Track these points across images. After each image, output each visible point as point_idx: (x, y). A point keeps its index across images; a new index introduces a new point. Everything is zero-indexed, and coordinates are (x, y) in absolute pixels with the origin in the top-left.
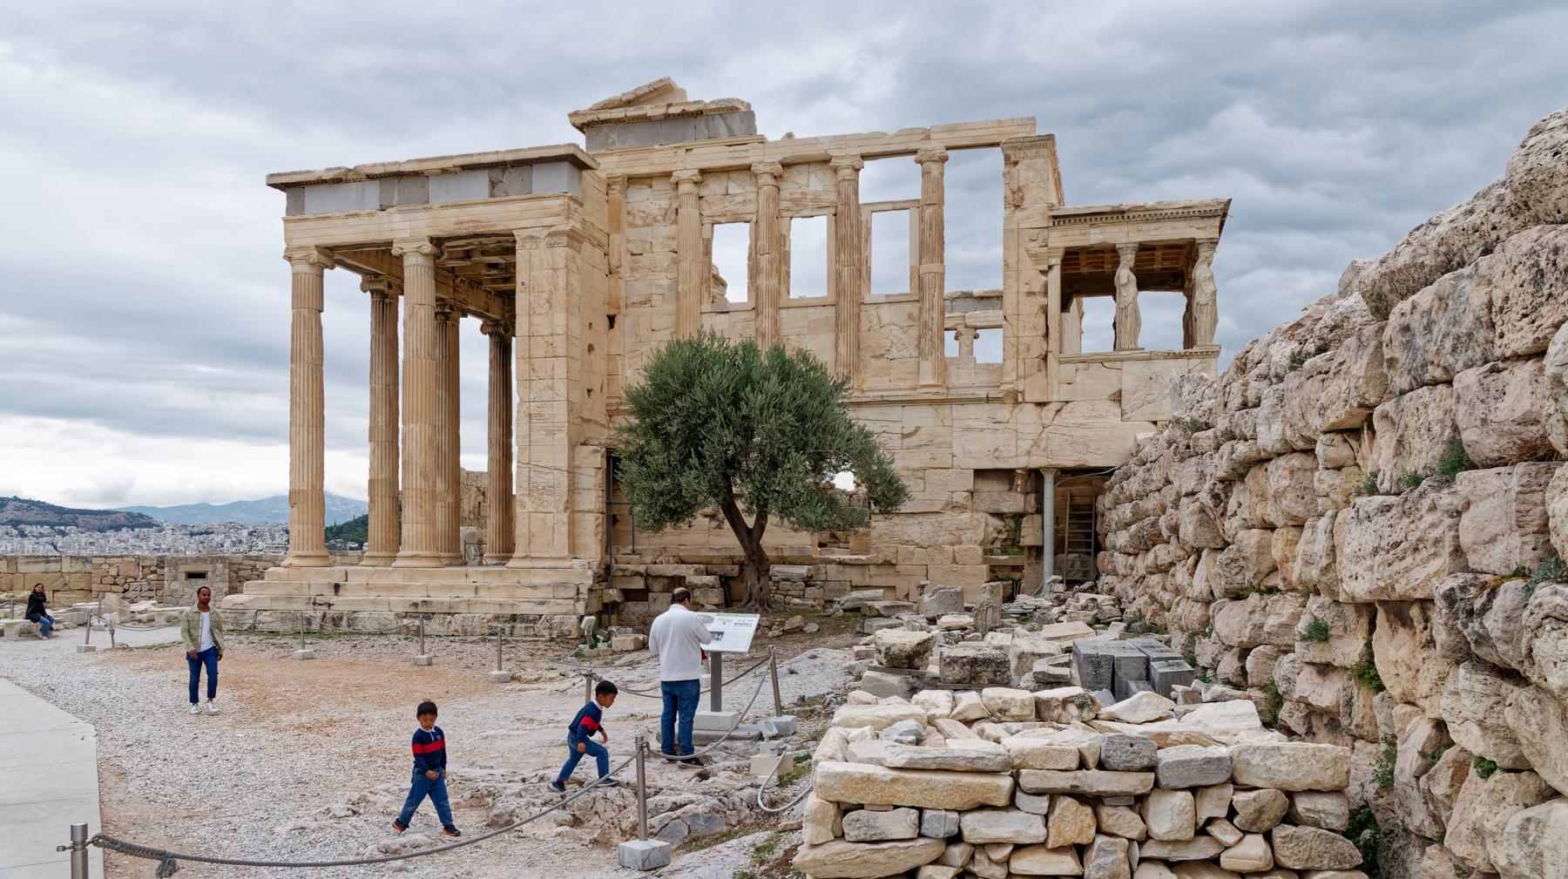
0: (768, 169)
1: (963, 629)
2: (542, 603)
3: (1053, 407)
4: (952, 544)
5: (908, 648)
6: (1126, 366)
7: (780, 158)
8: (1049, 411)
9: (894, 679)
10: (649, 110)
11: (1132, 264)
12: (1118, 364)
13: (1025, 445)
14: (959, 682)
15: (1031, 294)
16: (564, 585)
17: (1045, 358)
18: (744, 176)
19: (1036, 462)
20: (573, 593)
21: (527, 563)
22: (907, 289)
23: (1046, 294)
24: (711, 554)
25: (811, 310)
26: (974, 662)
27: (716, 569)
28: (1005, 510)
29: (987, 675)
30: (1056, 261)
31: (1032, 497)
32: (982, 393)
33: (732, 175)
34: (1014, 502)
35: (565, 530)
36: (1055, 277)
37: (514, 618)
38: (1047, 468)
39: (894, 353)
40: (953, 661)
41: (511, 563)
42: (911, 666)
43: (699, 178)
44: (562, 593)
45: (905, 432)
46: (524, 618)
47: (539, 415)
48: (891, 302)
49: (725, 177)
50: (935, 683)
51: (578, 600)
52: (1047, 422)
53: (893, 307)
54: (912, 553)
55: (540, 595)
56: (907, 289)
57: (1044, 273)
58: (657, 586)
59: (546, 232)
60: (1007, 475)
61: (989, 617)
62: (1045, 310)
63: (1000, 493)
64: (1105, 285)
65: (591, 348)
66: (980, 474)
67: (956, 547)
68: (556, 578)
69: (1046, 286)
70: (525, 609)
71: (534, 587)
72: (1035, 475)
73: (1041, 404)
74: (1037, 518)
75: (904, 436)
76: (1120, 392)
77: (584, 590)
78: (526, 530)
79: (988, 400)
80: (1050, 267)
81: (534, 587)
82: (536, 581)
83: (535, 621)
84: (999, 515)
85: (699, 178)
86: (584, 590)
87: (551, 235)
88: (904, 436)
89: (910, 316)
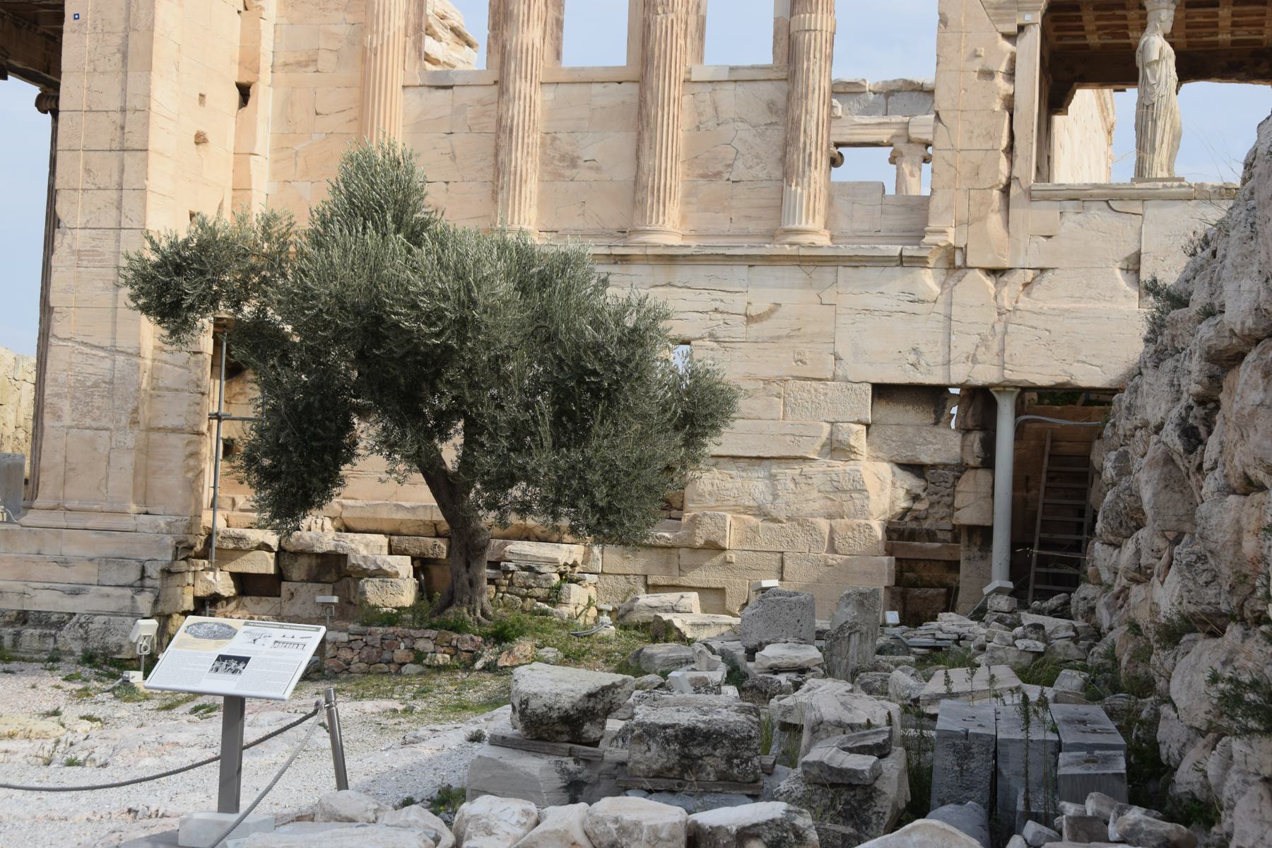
1: (802, 670)
2: (75, 593)
3: (1017, 279)
4: (830, 517)
5: (565, 703)
6: (1152, 211)
8: (1010, 290)
9: (535, 766)
11: (1168, 28)
12: (1136, 207)
13: (963, 345)
14: (658, 775)
16: (120, 561)
19: (984, 375)
20: (133, 576)
21: (58, 519)
22: (768, 59)
23: (1011, 75)
24: (400, 516)
25: (597, 88)
26: (689, 735)
27: (406, 543)
28: (926, 459)
29: (713, 763)
31: (976, 438)
32: (895, 250)
34: (944, 443)
35: (127, 460)
36: (1030, 48)
37: (23, 618)
38: (1004, 387)
39: (740, 171)
40: (649, 732)
41: (30, 518)
42: (577, 738)
44: (115, 575)
45: (753, 311)
46: (42, 620)
48: (738, 77)
50: (622, 781)
51: (141, 589)
52: (1007, 304)
53: (740, 89)
54: (755, 530)
55: (74, 576)
56: (768, 59)
58: (298, 570)
60: (931, 397)
61: (853, 651)
62: (1010, 104)
63: (918, 427)
64: (1119, 68)
65: (200, 139)
66: (882, 392)
67: (837, 522)
68: (109, 547)
69: (1013, 61)
70: (45, 601)
71: (65, 563)
72: (981, 399)
73: (995, 272)
74: (983, 475)
75: (750, 319)
76: (1138, 255)
77: (153, 570)
78: (59, 458)
79: (901, 261)
80: (1021, 28)
81: (65, 563)
82: (72, 551)
83: (60, 625)
84: (915, 469)
86: (153, 570)
88: (750, 319)
89: (771, 106)
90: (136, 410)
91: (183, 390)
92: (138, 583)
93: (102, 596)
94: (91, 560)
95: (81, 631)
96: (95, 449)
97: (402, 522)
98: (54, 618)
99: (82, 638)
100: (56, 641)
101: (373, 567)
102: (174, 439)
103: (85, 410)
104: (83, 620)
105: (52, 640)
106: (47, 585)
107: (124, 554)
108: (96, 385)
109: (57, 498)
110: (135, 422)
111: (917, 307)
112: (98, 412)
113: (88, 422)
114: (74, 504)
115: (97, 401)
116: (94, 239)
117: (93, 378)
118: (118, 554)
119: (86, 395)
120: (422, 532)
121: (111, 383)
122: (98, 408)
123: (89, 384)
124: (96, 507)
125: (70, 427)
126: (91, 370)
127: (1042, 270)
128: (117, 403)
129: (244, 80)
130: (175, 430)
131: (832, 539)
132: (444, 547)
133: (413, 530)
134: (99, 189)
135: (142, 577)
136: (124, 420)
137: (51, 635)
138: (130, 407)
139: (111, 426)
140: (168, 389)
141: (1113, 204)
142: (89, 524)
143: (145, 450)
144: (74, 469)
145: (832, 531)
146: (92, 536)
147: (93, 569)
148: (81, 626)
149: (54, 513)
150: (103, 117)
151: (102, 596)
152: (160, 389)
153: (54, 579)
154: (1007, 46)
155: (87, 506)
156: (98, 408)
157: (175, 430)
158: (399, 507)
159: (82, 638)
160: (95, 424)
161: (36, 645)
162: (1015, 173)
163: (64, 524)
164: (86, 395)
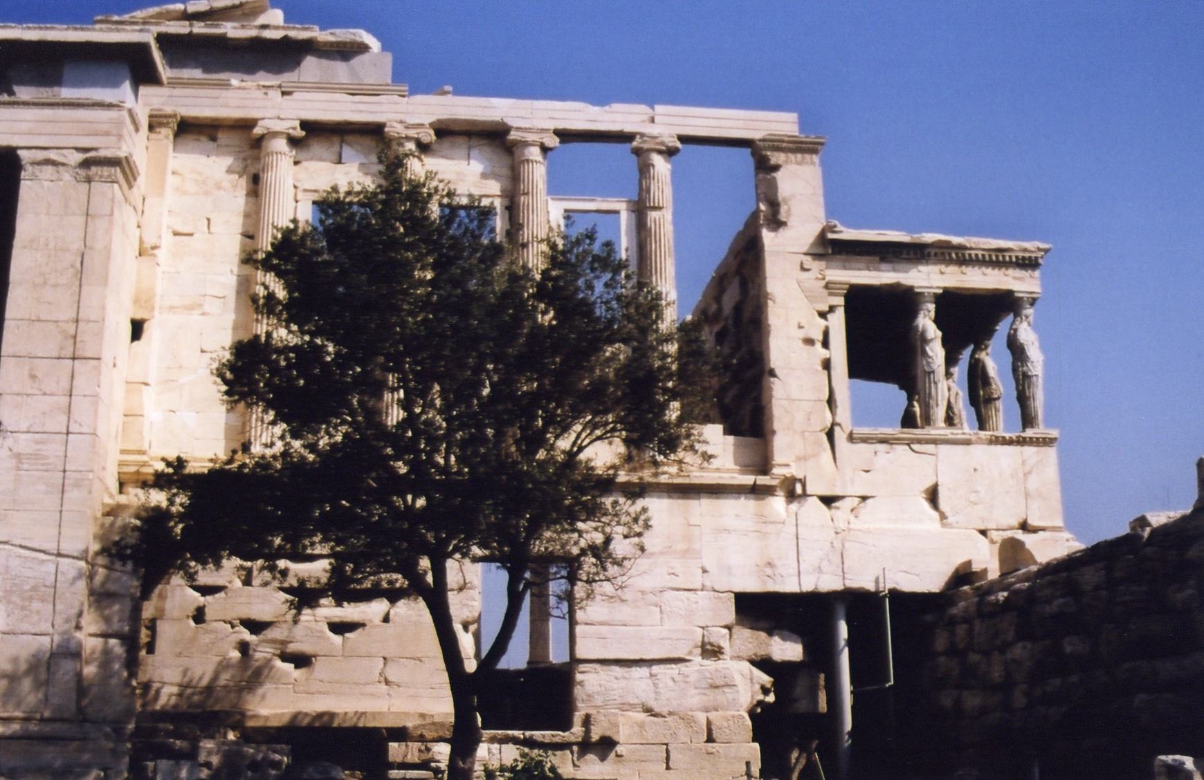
0: (412, 133)
7: (433, 119)
10: (231, 30)
12: (930, 448)
15: (809, 342)
17: (830, 435)
18: (368, 142)
23: (826, 344)
30: (840, 301)
33: (349, 138)
43: (300, 133)
47: (36, 456)
49: (336, 140)
57: (823, 315)
59: (80, 157)
62: (827, 365)
69: (826, 334)
73: (828, 501)
80: (832, 309)
85: (300, 133)
87: (86, 164)
108: (34, 589)
111: (770, 528)
113: (26, 627)
116: (37, 443)
117: (32, 582)
123: (27, 587)
126: (29, 573)
127: (864, 498)
129: (138, 316)
131: (710, 731)
134: (45, 394)
141: (915, 447)
145: (709, 723)
150: (51, 326)
154: (822, 322)
162: (838, 420)
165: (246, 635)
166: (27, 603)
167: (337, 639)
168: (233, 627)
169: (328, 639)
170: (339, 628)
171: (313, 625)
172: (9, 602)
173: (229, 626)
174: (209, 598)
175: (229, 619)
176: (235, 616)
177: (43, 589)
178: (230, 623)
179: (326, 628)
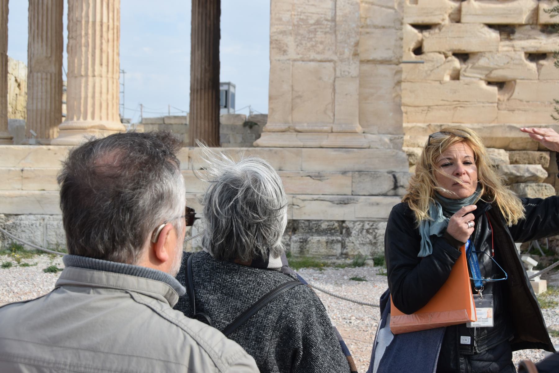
2: (343, 203)
20: (387, 185)
44: (368, 186)
68: (348, 161)
71: (319, 177)
90: (357, 44)
91: (389, 27)
92: (392, 192)
93: (372, 204)
94: (344, 173)
95: (370, 237)
96: (320, 79)
97: (514, 140)
98: (324, 226)
99: (371, 243)
100: (343, 246)
101: (527, 175)
102: (383, 69)
103: (309, 45)
104: (367, 226)
105: (339, 245)
106: (316, 197)
107: (363, 167)
108: (318, 23)
109: (286, 122)
110: (356, 54)
112: (321, 47)
113: (313, 55)
114: (305, 127)
115: (320, 36)
117: (315, 17)
118: (357, 167)
119: (310, 32)
120: (528, 147)
121: (334, 20)
122: (322, 43)
123: (312, 22)
124: (325, 128)
125: (295, 60)
126: (313, 10)
128: (340, 38)
130: (383, 62)
132: (548, 157)
133: (521, 146)
135: (396, 187)
136: (347, 53)
137: (338, 241)
138: (352, 41)
139: (335, 58)
140: (376, 27)
142: (325, 143)
143: (363, 80)
144: (300, 97)
146: (332, 153)
147: (346, 181)
148: (368, 231)
149: (287, 135)
151: (372, 204)
152: (368, 26)
153: (308, 192)
155: (317, 128)
156: (322, 43)
157: (383, 62)
158: (512, 128)
159: (371, 243)
160: (319, 57)
161: (323, 250)
163: (301, 144)
164: (310, 32)
165: (457, 63)
166: (312, 36)
167: (533, 65)
168: (446, 57)
169: (526, 65)
170: (535, 56)
171: (512, 54)
172: (297, 34)
173: (442, 56)
174: (426, 33)
175: (443, 50)
176: (447, 47)
177: (325, 23)
178: (444, 54)
179: (523, 56)
